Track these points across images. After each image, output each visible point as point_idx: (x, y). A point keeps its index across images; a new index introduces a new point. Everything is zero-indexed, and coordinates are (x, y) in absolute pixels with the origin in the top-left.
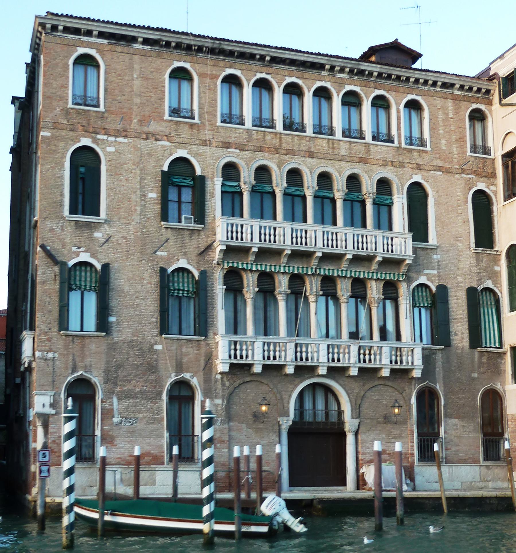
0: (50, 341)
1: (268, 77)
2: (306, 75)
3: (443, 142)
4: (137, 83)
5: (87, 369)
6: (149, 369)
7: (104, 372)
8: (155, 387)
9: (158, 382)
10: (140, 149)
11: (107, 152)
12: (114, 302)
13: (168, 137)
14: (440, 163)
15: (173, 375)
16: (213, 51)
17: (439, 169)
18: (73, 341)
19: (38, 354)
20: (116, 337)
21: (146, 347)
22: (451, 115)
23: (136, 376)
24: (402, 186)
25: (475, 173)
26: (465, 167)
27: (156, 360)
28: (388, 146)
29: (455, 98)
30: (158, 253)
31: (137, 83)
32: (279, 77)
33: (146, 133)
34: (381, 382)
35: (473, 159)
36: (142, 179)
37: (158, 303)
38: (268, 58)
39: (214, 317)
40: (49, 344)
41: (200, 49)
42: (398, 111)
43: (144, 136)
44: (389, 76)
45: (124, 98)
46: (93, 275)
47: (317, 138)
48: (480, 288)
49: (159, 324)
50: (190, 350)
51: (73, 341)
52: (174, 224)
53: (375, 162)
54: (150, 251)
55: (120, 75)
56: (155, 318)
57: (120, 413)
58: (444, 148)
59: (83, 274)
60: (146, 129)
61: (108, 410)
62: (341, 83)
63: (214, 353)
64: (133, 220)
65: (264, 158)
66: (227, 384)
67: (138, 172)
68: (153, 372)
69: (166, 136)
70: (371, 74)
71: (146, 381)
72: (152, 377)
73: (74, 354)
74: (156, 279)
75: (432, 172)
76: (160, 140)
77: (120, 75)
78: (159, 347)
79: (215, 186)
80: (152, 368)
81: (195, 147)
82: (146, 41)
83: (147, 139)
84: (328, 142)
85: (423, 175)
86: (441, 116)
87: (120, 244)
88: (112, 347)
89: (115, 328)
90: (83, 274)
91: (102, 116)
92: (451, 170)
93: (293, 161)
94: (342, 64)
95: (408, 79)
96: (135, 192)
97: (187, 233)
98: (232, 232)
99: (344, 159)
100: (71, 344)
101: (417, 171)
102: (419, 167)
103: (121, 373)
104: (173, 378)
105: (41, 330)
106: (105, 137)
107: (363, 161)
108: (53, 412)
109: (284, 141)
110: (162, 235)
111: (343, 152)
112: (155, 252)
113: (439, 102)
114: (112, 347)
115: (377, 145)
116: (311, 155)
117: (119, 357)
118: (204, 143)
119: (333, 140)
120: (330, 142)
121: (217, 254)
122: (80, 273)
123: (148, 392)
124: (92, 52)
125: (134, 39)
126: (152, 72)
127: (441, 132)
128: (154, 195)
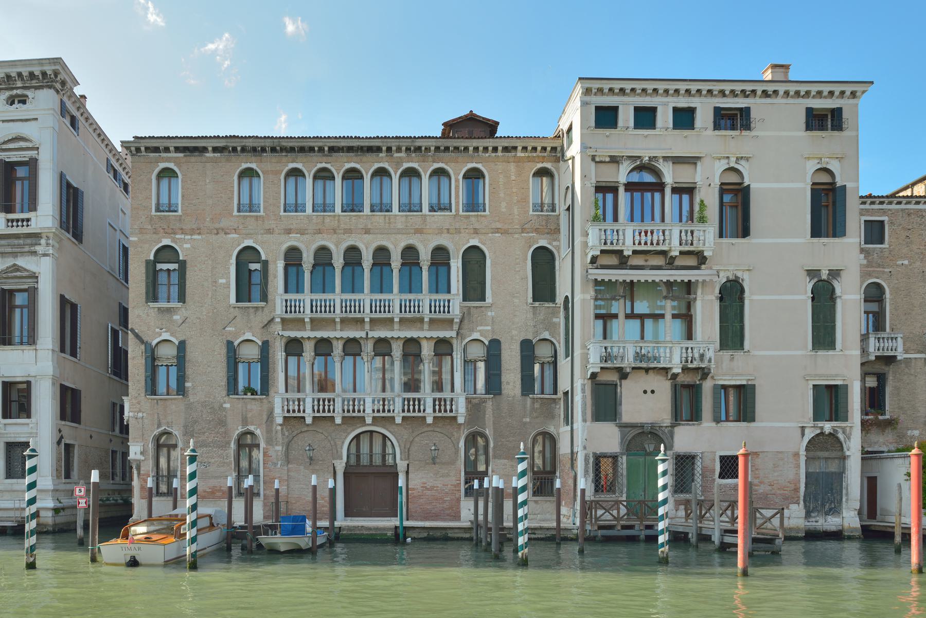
3: (504, 204)
12: (189, 371)
13: (236, 230)
16: (273, 150)
20: (192, 398)
24: (458, 251)
34: (430, 429)
41: (263, 150)
56: (224, 382)
60: (217, 226)
79: (278, 268)
81: (260, 236)
83: (217, 234)
92: (510, 231)
99: (399, 232)
107: (419, 231)
111: (400, 226)
125: (204, 150)
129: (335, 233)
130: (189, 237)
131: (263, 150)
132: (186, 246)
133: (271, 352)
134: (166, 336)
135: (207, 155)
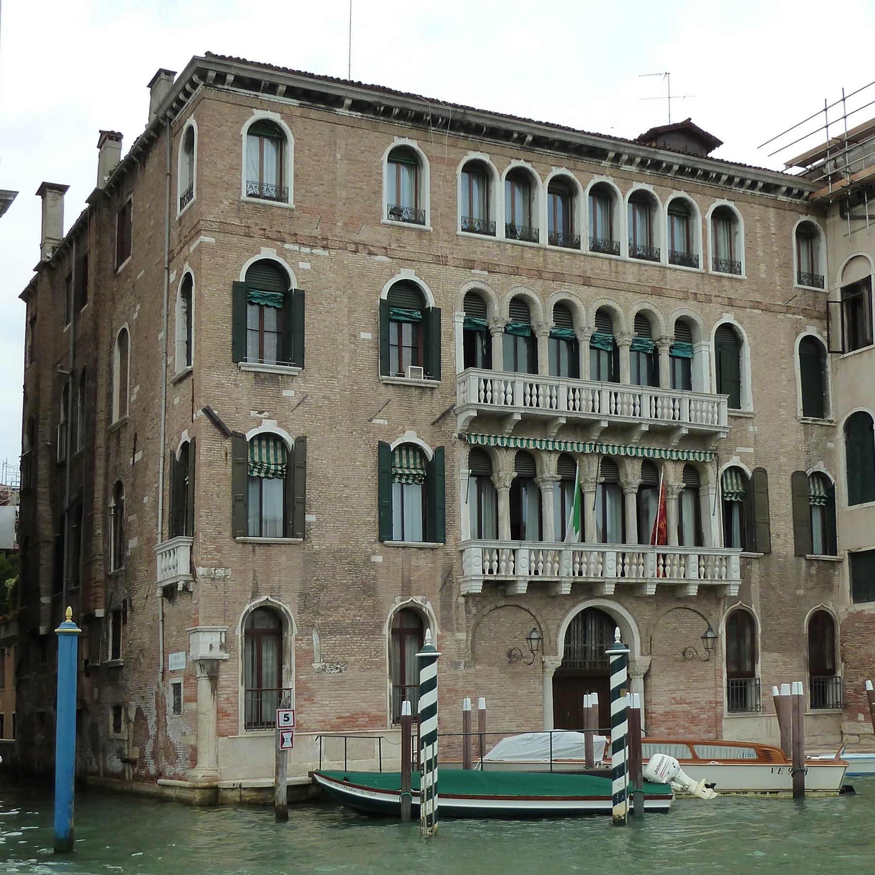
0: (220, 552)
1: (528, 166)
2: (580, 165)
3: (763, 267)
4: (342, 167)
5: (271, 591)
6: (364, 591)
7: (299, 596)
8: (372, 617)
9: (377, 609)
11: (299, 269)
12: (312, 494)
15: (398, 599)
17: (756, 305)
18: (254, 551)
19: (200, 571)
20: (316, 543)
21: (358, 560)
22: (773, 230)
23: (346, 601)
25: (804, 312)
26: (790, 304)
27: (375, 578)
28: (690, 272)
29: (779, 206)
30: (375, 421)
31: (342, 167)
32: (543, 167)
33: (355, 243)
35: (800, 293)
36: (351, 311)
37: (374, 495)
38: (530, 138)
39: (456, 515)
40: (218, 556)
42: (704, 222)
43: (352, 247)
44: (694, 173)
46: (279, 453)
47: (595, 257)
49: (377, 525)
50: (422, 562)
51: (254, 551)
52: (393, 378)
53: (674, 294)
55: (316, 154)
56: (373, 517)
57: (322, 656)
58: (763, 276)
59: (264, 451)
60: (356, 238)
61: (306, 651)
62: (628, 179)
63: (456, 567)
64: (339, 372)
65: (523, 285)
66: (474, 610)
67: (346, 300)
68: (370, 595)
69: (385, 248)
70: (669, 168)
71: (361, 607)
72: (369, 602)
73: (255, 571)
74: (372, 460)
75: (748, 310)
76: (376, 255)
77: (316, 154)
78: (379, 559)
80: (368, 589)
82: (357, 105)
83: (356, 252)
84: (610, 263)
85: (736, 315)
86: (759, 231)
87: (320, 407)
88: (311, 560)
89: (314, 532)
90: (264, 451)
93: (563, 290)
94: (633, 152)
95: (719, 176)
96: (341, 331)
97: (416, 392)
98: (486, 391)
100: (251, 556)
101: (729, 308)
102: (731, 303)
103: (324, 597)
104: (398, 604)
105: (205, 536)
106: (296, 248)
107: (657, 292)
108: (226, 656)
109: (549, 261)
110: (380, 395)
111: (630, 279)
112: (370, 421)
113: (757, 210)
114: (311, 560)
115: (675, 270)
116: (587, 282)
118: (440, 260)
119: (617, 260)
120: (613, 263)
121: (460, 423)
122: (260, 451)
123: (363, 624)
124: (276, 117)
126: (363, 152)
127: (760, 253)
128: (366, 336)
132: (302, 265)
133: (447, 466)
135: (340, 111)
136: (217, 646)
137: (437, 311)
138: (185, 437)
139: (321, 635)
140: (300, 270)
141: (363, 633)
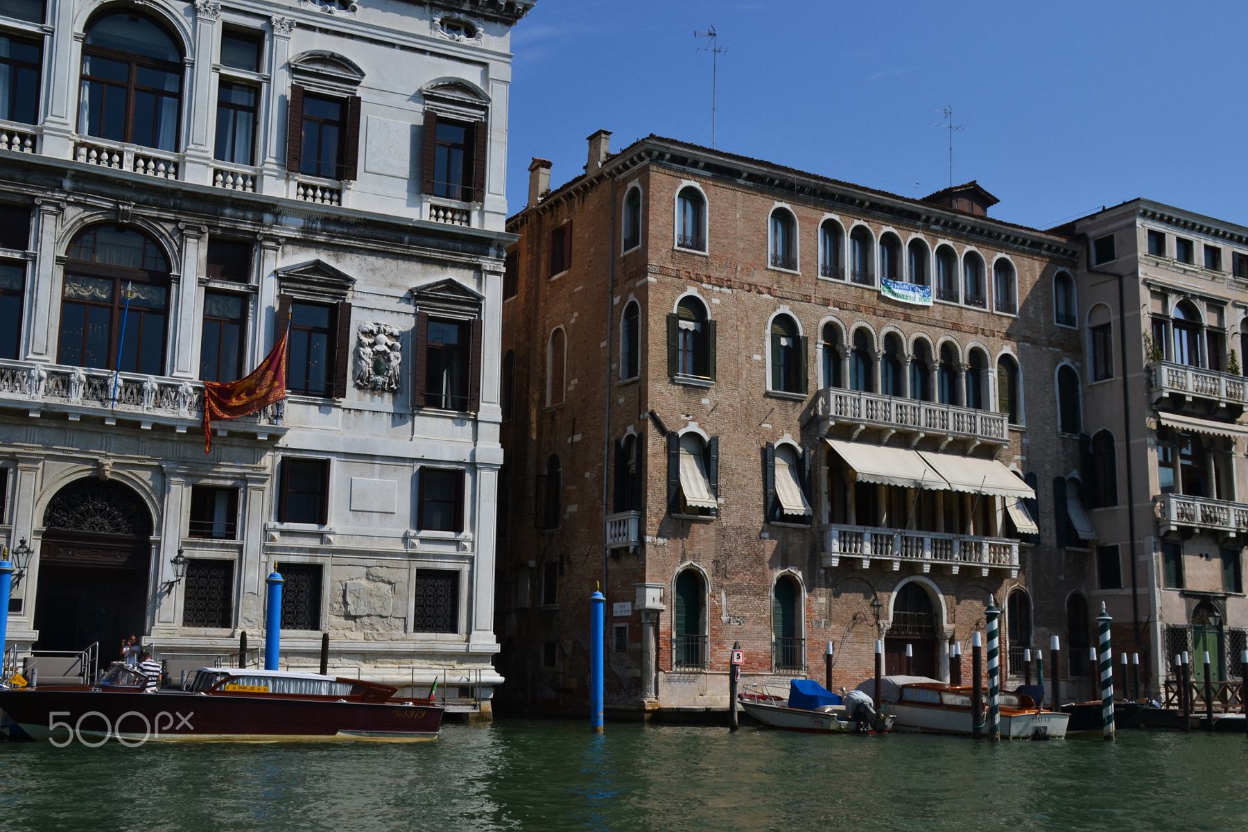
10: (743, 303)
14: (1029, 334)
23: (744, 568)
36: (747, 338)
42: (990, 271)
43: (746, 287)
45: (726, 241)
48: (1067, 478)
53: (967, 329)
54: (755, 423)
60: (750, 280)
83: (749, 291)
88: (722, 533)
91: (707, 262)
107: (956, 327)
114: (722, 533)
117: (727, 546)
129: (875, 314)
130: (717, 289)
131: (802, 190)
132: (716, 301)
134: (693, 427)
136: (658, 599)
137: (806, 339)
138: (631, 430)
139: (727, 595)
140: (714, 303)
141: (756, 594)
